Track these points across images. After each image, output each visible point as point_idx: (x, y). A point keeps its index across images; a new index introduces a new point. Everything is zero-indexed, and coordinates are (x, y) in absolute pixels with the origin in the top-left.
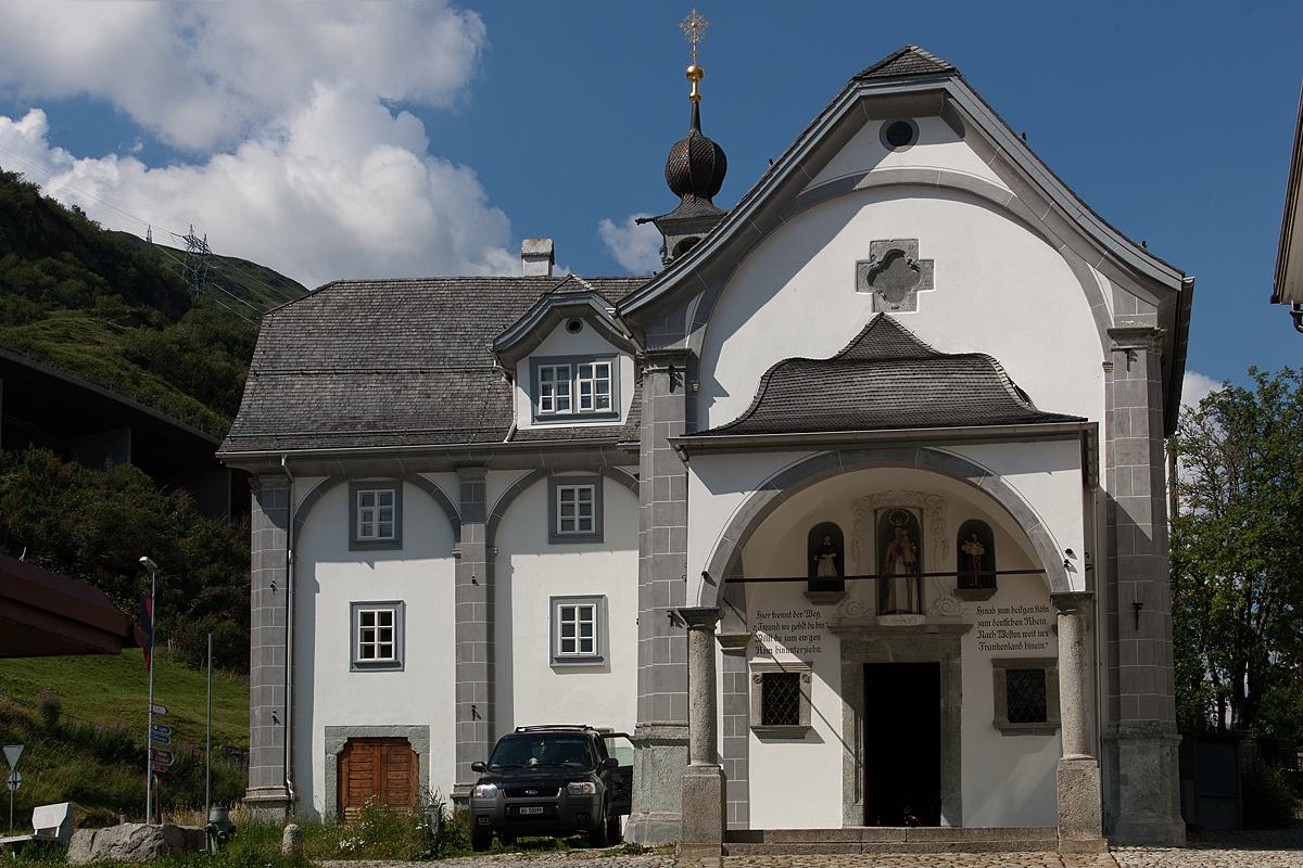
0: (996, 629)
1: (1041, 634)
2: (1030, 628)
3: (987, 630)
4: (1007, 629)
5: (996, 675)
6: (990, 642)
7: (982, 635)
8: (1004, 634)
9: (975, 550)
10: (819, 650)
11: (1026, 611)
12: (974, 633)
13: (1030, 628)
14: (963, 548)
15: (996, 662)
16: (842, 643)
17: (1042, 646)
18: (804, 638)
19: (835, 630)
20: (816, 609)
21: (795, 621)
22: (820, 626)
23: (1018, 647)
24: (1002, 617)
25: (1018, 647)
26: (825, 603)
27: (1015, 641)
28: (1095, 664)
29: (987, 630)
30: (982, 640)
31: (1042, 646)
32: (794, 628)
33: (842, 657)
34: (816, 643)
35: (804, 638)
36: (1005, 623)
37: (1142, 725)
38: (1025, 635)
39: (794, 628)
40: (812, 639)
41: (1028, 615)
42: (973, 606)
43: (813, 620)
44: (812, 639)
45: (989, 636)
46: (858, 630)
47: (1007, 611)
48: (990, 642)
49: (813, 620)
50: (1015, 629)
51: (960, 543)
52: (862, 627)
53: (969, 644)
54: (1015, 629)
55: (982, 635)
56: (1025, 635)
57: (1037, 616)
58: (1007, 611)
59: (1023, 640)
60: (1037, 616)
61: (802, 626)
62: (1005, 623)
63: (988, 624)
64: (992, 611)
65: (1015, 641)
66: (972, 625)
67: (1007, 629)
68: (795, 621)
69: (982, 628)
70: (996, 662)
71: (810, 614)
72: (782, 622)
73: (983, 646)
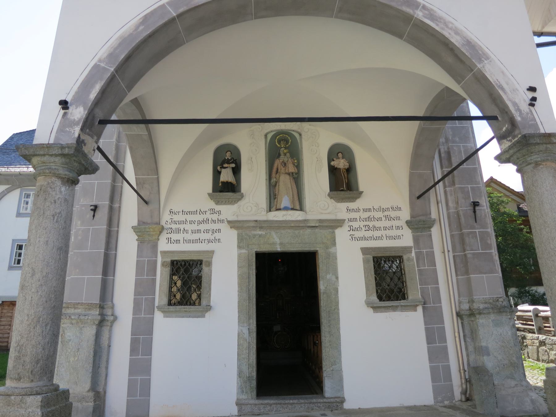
0: (362, 224)
1: (398, 228)
2: (388, 224)
3: (355, 225)
4: (371, 224)
5: (365, 261)
6: (358, 234)
7: (351, 229)
8: (368, 228)
9: (341, 164)
10: (219, 240)
11: (384, 210)
12: (346, 228)
13: (388, 224)
14: (332, 163)
15: (365, 251)
16: (239, 235)
17: (399, 237)
18: (207, 231)
19: (233, 224)
20: (218, 208)
21: (200, 217)
22: (222, 221)
23: (380, 238)
24: (366, 215)
25: (380, 238)
26: (225, 203)
27: (377, 234)
28: (444, 252)
29: (355, 225)
30: (352, 232)
31: (399, 237)
32: (200, 223)
33: (239, 247)
34: (217, 235)
35: (207, 231)
36: (369, 219)
37: (491, 301)
38: (385, 228)
39: (200, 223)
40: (214, 232)
41: (386, 213)
42: (343, 206)
43: (215, 217)
44: (214, 232)
45: (357, 229)
46: (252, 224)
47: (369, 210)
48: (358, 234)
49: (215, 217)
50: (377, 224)
51: (330, 160)
52: (256, 221)
53: (341, 234)
54: (377, 224)
55: (351, 229)
56: (385, 228)
57: (393, 214)
58: (369, 210)
59: (383, 233)
60: (393, 214)
61: (206, 221)
62: (369, 219)
63: (355, 220)
64: (358, 210)
65: (377, 234)
66: (345, 220)
67: (371, 224)
68: (200, 217)
69: (351, 224)
70: (365, 251)
71: (213, 211)
72: (190, 217)
73: (352, 238)
